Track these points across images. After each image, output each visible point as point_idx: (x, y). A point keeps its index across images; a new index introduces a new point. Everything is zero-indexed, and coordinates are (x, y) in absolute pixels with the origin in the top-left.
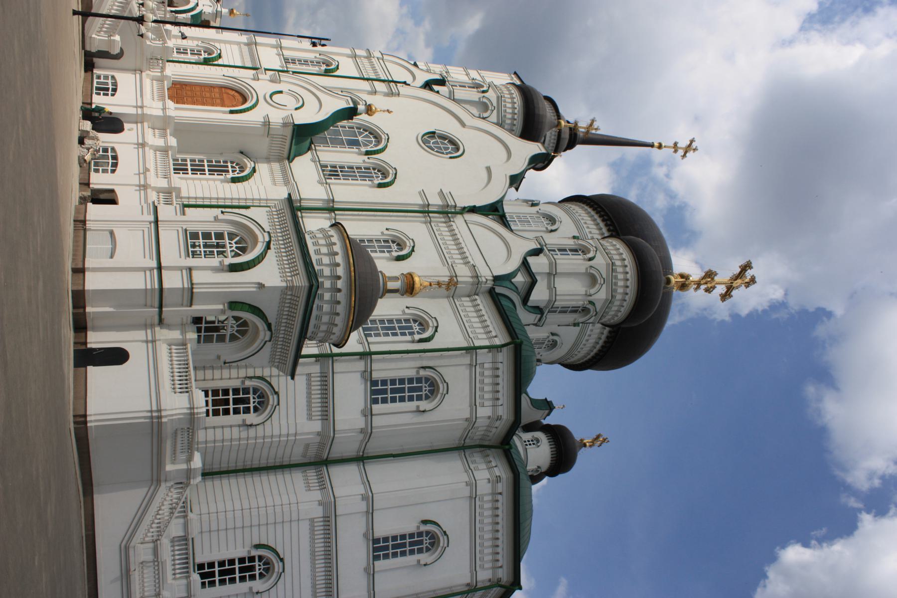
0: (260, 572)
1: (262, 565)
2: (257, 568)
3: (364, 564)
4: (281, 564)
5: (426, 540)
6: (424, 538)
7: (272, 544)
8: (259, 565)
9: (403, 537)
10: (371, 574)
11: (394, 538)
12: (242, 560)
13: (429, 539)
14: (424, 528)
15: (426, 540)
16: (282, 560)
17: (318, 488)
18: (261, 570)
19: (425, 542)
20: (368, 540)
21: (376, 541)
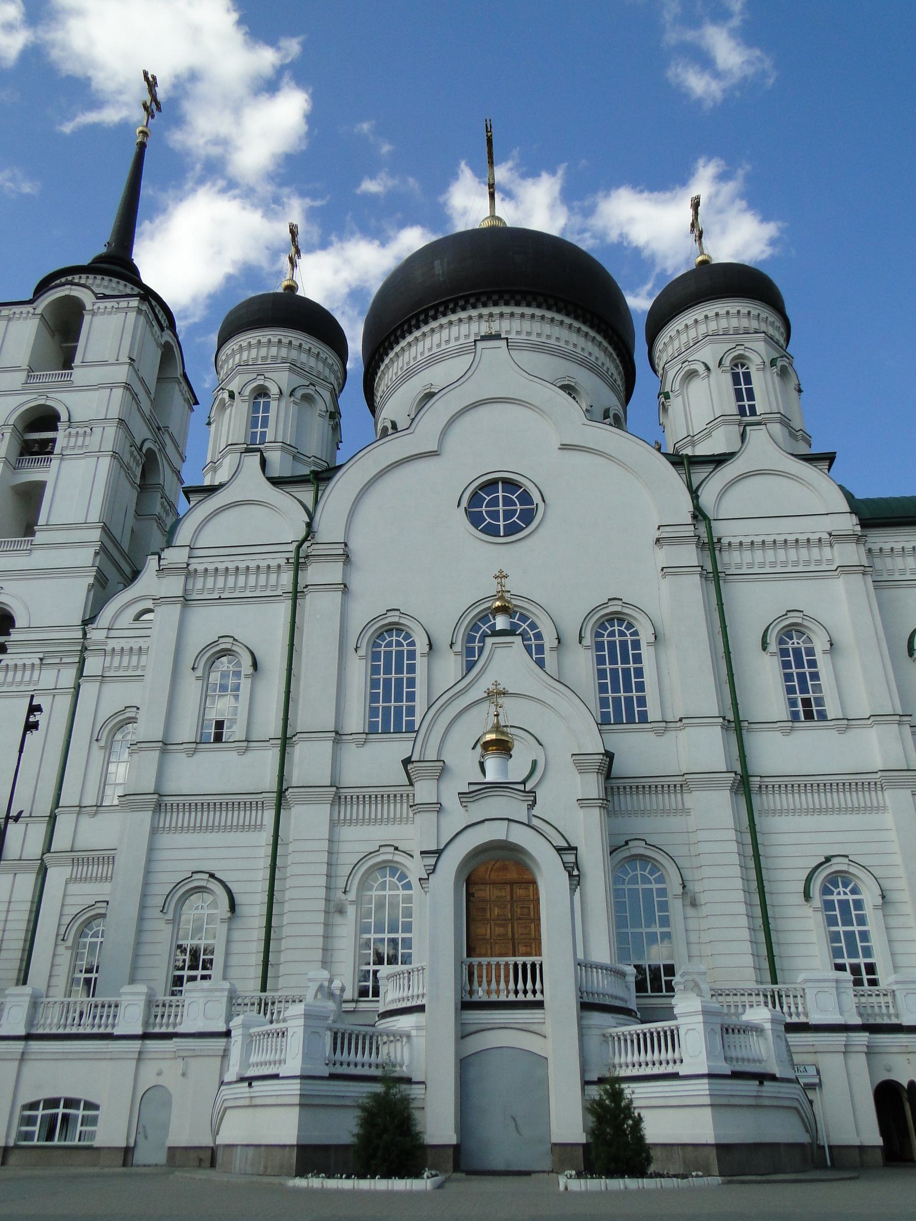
0: (849, 893)
1: (838, 890)
2: (842, 897)
3: (652, 735)
4: (834, 860)
5: (793, 643)
6: (790, 646)
7: (804, 874)
8: (839, 893)
9: (788, 677)
10: (847, 723)
11: (790, 690)
12: (831, 921)
13: (791, 639)
14: (773, 647)
15: (793, 643)
16: (828, 859)
17: (260, 812)
18: (847, 891)
19: (796, 645)
20: (792, 729)
21: (795, 717)
